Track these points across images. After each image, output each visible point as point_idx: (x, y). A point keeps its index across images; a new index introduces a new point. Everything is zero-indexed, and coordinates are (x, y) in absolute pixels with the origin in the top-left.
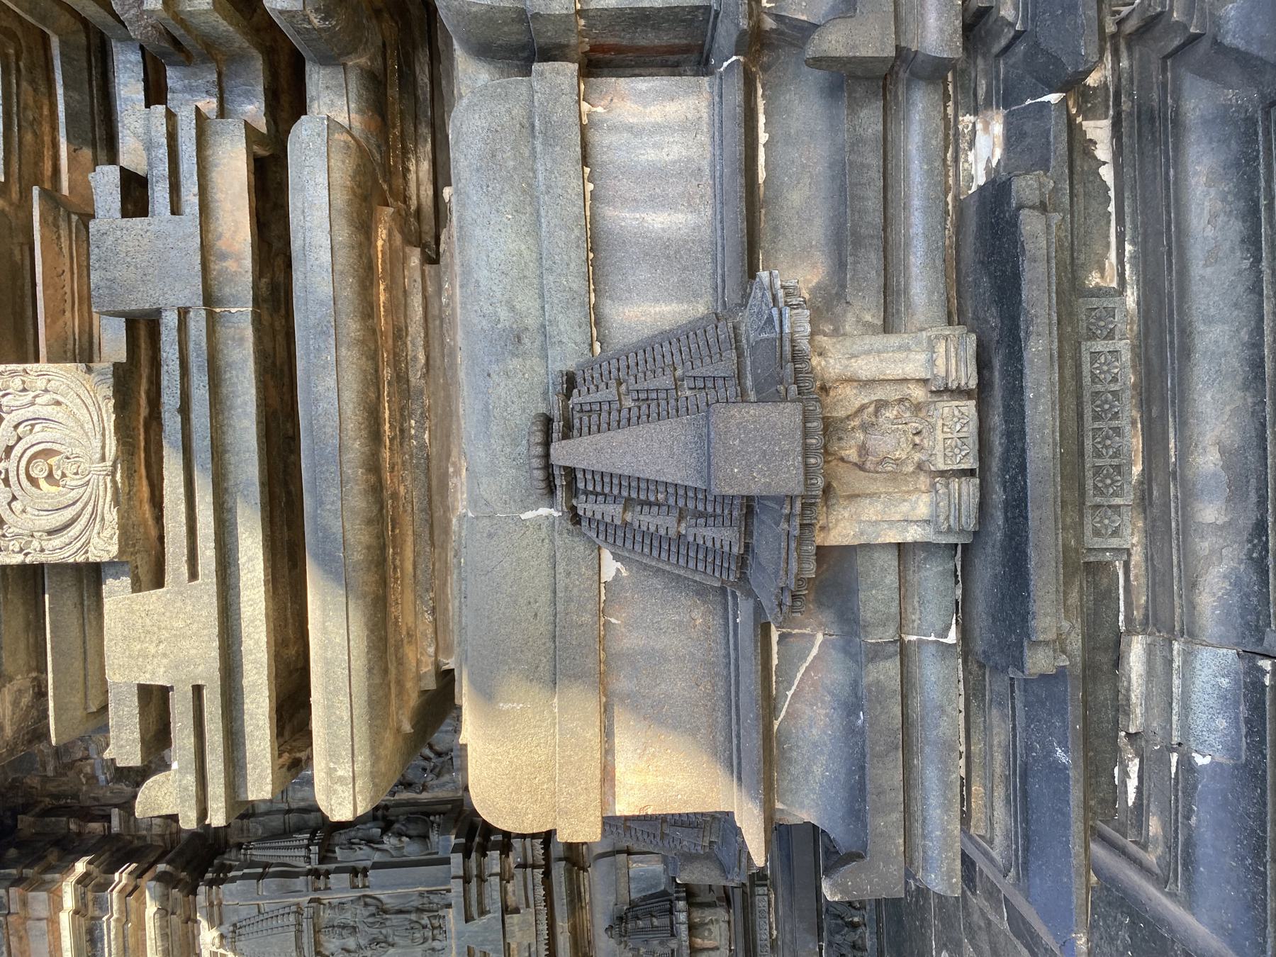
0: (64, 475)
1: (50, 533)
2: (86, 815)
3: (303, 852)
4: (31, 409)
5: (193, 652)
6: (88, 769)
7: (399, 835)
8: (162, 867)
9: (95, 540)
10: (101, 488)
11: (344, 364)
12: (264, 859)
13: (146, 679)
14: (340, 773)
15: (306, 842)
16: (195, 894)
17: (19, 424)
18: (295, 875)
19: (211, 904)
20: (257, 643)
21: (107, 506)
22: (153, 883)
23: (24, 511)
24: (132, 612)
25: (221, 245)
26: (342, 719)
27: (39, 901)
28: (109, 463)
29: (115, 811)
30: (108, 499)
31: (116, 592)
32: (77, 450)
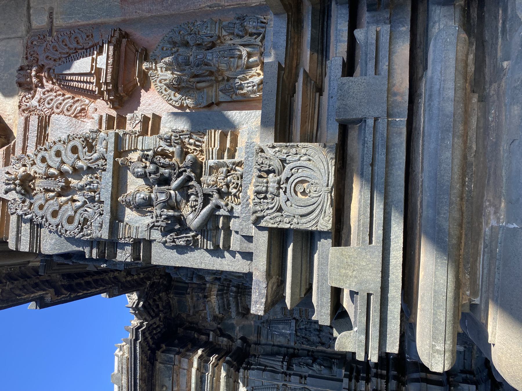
0: (310, 192)
1: (302, 216)
2: (200, 332)
3: (280, 364)
4: (299, 162)
5: (369, 277)
6: (203, 315)
7: (320, 365)
8: (228, 358)
9: (321, 221)
10: (326, 198)
11: (456, 146)
12: (265, 363)
13: (334, 285)
14: (437, 348)
15: (281, 360)
16: (239, 372)
17: (293, 168)
18: (278, 373)
19: (244, 377)
20: (397, 277)
21: (328, 207)
22: (225, 364)
23: (291, 206)
24: (342, 255)
25: (395, 89)
26: (441, 321)
27: (185, 361)
28: (330, 188)
29: (211, 333)
30: (329, 203)
31: (324, 245)
32: (317, 181)
